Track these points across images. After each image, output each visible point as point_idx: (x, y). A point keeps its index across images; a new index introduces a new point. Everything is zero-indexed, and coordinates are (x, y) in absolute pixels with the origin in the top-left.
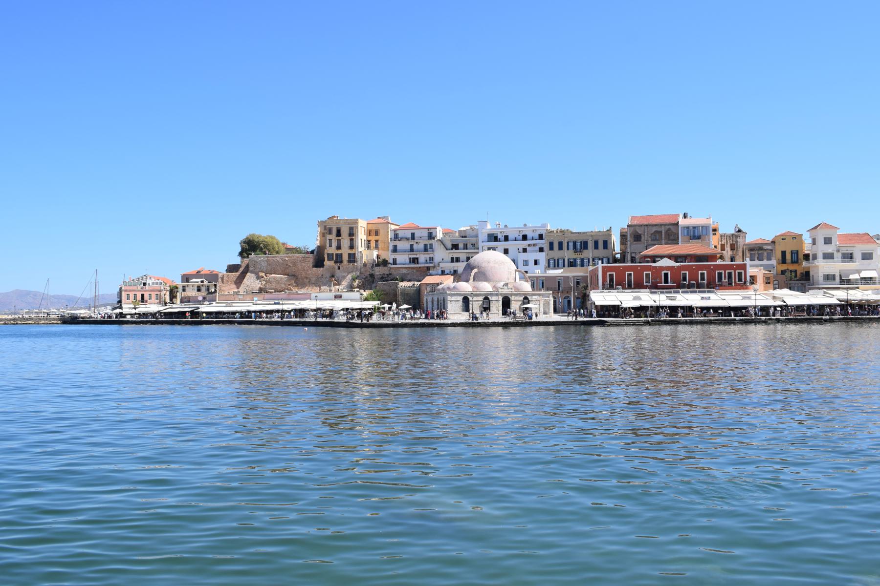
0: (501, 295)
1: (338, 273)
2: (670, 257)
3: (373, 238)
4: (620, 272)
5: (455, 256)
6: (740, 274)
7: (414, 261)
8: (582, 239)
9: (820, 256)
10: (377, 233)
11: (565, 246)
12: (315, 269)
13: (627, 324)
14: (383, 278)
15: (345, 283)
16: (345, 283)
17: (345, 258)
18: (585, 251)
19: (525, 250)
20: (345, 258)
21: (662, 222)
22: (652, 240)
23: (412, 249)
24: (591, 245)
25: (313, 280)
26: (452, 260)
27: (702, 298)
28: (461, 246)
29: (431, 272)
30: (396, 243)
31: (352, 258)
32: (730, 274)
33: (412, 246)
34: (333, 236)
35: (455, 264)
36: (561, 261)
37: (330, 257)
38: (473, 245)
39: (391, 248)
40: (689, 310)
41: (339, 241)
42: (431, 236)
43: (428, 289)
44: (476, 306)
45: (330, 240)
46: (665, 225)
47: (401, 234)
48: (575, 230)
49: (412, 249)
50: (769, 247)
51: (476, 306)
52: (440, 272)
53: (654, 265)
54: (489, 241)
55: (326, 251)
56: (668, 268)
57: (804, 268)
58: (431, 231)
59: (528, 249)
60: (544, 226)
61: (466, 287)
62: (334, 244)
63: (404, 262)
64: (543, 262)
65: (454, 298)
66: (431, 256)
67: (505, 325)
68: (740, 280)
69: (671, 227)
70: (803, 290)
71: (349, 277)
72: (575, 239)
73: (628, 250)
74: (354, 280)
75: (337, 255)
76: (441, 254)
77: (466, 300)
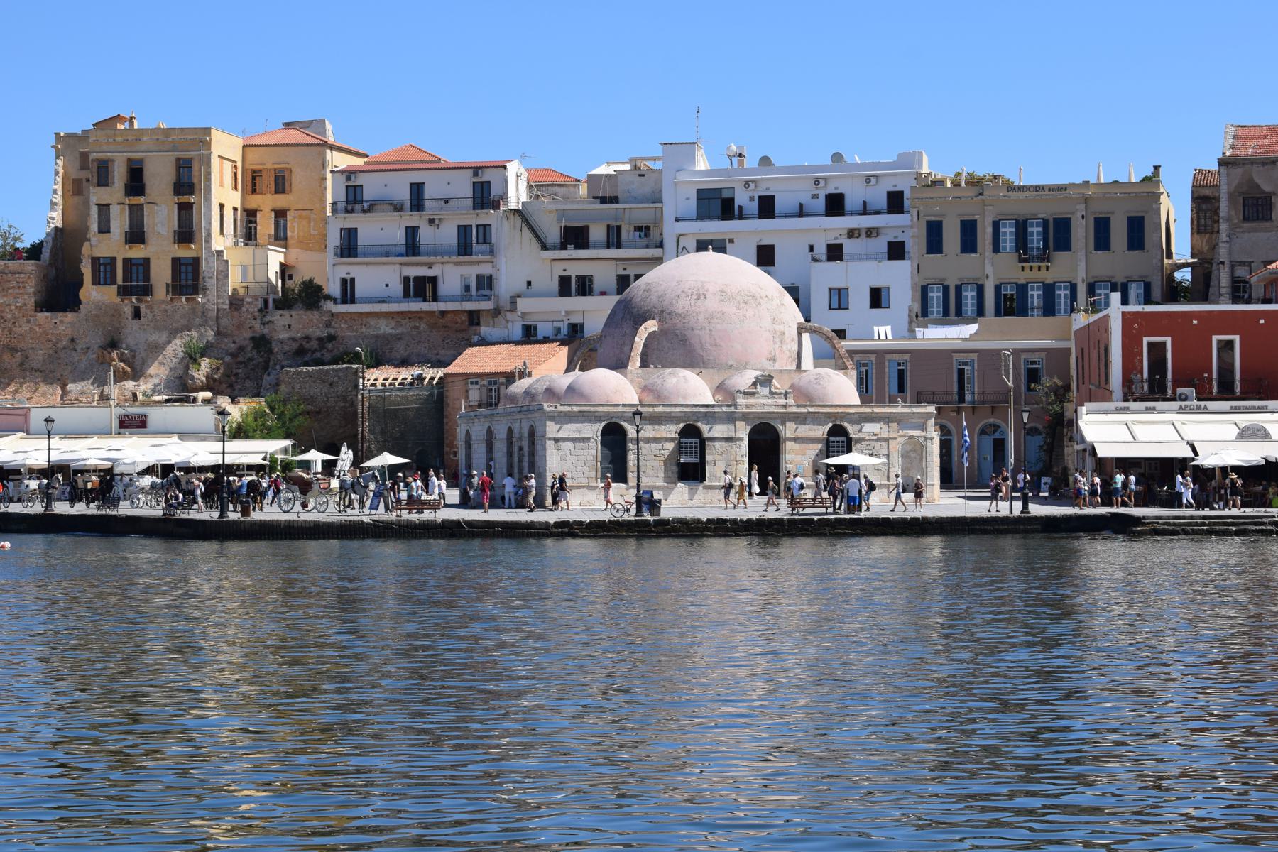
0: (745, 417)
1: (134, 334)
3: (266, 203)
4: (1192, 335)
5: (574, 271)
7: (422, 288)
8: (1049, 210)
10: (281, 183)
12: (43, 316)
13: (1218, 530)
14: (302, 353)
15: (158, 372)
16: (158, 372)
17: (161, 274)
18: (1061, 257)
19: (835, 253)
20: (161, 274)
23: (412, 246)
24: (1081, 233)
25: (38, 356)
26: (565, 287)
28: (597, 233)
29: (484, 330)
31: (188, 277)
33: (412, 232)
34: (114, 194)
35: (576, 304)
36: (969, 295)
38: (643, 230)
39: (334, 239)
41: (136, 214)
42: (485, 195)
43: (475, 395)
44: (651, 457)
47: (372, 188)
49: (412, 246)
51: (651, 457)
52: (517, 332)
54: (700, 217)
55: (86, 249)
58: (486, 176)
59: (849, 246)
60: (908, 160)
61: (614, 388)
62: (119, 222)
63: (385, 292)
64: (902, 298)
65: (569, 430)
66: (486, 270)
71: (176, 346)
72: (1023, 210)
73: (1223, 253)
74: (192, 357)
75: (127, 262)
76: (520, 265)
77: (615, 441)
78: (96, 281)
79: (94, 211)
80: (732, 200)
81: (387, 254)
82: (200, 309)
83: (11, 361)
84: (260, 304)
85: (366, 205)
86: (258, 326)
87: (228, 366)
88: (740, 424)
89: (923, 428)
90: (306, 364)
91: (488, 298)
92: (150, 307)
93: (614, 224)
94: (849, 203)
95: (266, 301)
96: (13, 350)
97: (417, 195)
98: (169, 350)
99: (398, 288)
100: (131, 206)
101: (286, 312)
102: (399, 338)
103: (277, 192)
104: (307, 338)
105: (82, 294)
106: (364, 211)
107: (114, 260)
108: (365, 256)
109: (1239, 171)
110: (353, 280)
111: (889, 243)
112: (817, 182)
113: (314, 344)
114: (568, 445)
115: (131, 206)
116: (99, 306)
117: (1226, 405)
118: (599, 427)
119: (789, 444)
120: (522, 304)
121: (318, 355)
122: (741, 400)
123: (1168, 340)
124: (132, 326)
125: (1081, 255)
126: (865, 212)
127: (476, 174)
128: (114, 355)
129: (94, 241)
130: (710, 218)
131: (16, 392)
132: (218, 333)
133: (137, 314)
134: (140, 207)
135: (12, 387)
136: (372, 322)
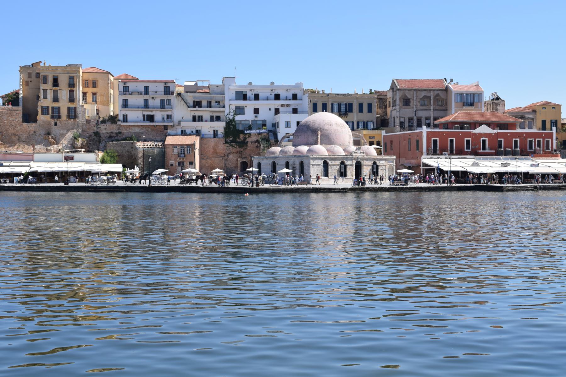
0: (355, 159)
1: (55, 131)
2: (489, 124)
3: (90, 90)
5: (197, 114)
6: (548, 142)
7: (151, 118)
8: (347, 101)
10: (94, 85)
11: (329, 107)
12: (25, 124)
13: (526, 189)
14: (111, 137)
15: (64, 142)
16: (64, 142)
17: (64, 112)
18: (350, 114)
20: (64, 112)
21: (430, 87)
22: (421, 105)
23: (146, 105)
24: (355, 108)
25: (24, 137)
26: (194, 119)
27: (532, 165)
28: (204, 103)
29: (169, 131)
30: (127, 97)
31: (73, 113)
32: (539, 141)
33: (146, 101)
34: (49, 86)
35: (198, 125)
37: (45, 110)
41: (56, 92)
42: (167, 91)
43: (176, 151)
47: (132, 86)
48: (334, 92)
49: (146, 105)
50: (531, 116)
52: (180, 132)
53: (474, 131)
54: (236, 99)
58: (168, 85)
59: (281, 109)
60: (298, 85)
62: (50, 95)
65: (316, 162)
66: (169, 113)
67: (344, 191)
68: (548, 148)
69: (439, 92)
71: (70, 135)
72: (340, 101)
74: (75, 138)
75: (53, 108)
76: (181, 112)
77: (326, 165)
78: (42, 114)
79: (42, 92)
81: (138, 108)
83: (15, 138)
84: (96, 122)
85: (130, 93)
87: (87, 141)
89: (393, 162)
90: (113, 141)
91: (171, 122)
92: (60, 122)
93: (209, 100)
94: (281, 97)
95: (98, 121)
96: (15, 135)
97: (146, 90)
98: (67, 136)
99: (142, 118)
102: (142, 133)
103: (93, 87)
104: (112, 133)
105: (38, 118)
106: (129, 94)
107: (48, 107)
108: (132, 108)
109: (402, 92)
110: (127, 115)
111: (293, 109)
112: (272, 90)
113: (115, 135)
114: (315, 166)
116: (43, 121)
117: (457, 157)
118: (322, 161)
120: (182, 124)
121: (116, 138)
122: (354, 154)
123: (438, 139)
124: (54, 128)
127: (166, 84)
128: (50, 137)
129: (42, 101)
130: (239, 100)
131: (17, 148)
132: (82, 131)
133: (56, 124)
134: (57, 91)
135: (16, 147)
136: (133, 128)
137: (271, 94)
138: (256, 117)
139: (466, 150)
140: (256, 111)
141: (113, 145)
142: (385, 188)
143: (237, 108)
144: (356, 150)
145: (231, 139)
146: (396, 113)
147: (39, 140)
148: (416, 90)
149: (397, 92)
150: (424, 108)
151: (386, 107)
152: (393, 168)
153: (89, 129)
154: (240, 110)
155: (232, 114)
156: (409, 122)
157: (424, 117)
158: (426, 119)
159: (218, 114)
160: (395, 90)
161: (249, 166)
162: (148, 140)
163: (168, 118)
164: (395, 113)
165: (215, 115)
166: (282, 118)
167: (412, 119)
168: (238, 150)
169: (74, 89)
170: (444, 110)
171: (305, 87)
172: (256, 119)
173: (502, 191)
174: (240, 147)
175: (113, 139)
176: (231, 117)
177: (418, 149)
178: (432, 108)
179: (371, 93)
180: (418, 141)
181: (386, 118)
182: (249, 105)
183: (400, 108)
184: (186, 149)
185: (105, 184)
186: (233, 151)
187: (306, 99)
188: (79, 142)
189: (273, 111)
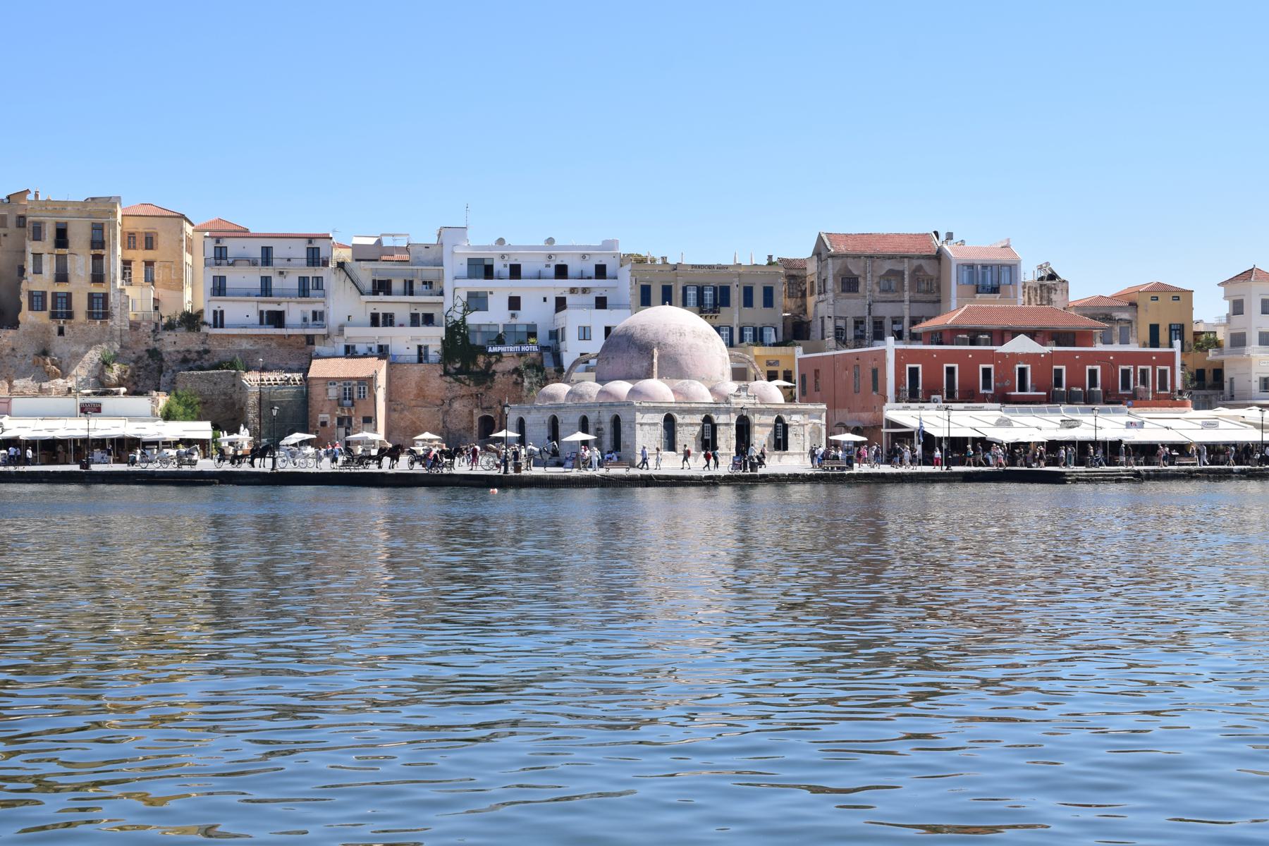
0: (735, 411)
1: (60, 346)
2: (1032, 334)
3: (139, 256)
5: (381, 310)
6: (1163, 373)
7: (276, 319)
9: (1253, 337)
10: (150, 243)
11: (677, 294)
14: (186, 361)
15: (81, 372)
16: (81, 372)
17: (80, 305)
18: (723, 309)
20: (80, 305)
21: (901, 250)
22: (882, 291)
23: (266, 289)
24: (736, 296)
26: (375, 321)
27: (1130, 425)
28: (397, 285)
29: (318, 348)
30: (223, 271)
31: (100, 307)
32: (1144, 372)
33: (266, 281)
34: (46, 246)
35: (382, 334)
37: (37, 301)
40: (1112, 449)
42: (314, 258)
43: (333, 392)
45: (38, 256)
46: (910, 257)
47: (234, 247)
48: (688, 261)
49: (266, 289)
50: (1125, 316)
52: (342, 350)
54: (470, 277)
56: (1027, 357)
57: (1212, 362)
58: (316, 244)
59: (570, 299)
60: (609, 245)
62: (49, 267)
63: (247, 321)
65: (648, 418)
66: (319, 307)
67: (711, 483)
68: (1163, 387)
69: (922, 262)
70: (1210, 408)
71: (93, 356)
72: (701, 281)
74: (105, 363)
75: (55, 295)
76: (344, 305)
77: (670, 423)
78: (31, 308)
79: (30, 258)
80: (492, 266)
81: (248, 295)
82: (108, 329)
84: (153, 327)
85: (231, 261)
86: (151, 342)
87: (132, 369)
88: (732, 415)
89: (820, 418)
90: (191, 369)
92: (72, 327)
93: (409, 279)
94: (570, 271)
95: (157, 325)
97: (267, 256)
98: (87, 357)
99: (256, 319)
100: (57, 255)
101: (172, 333)
102: (257, 352)
104: (189, 351)
105: (20, 317)
106: (229, 265)
107: (44, 294)
108: (233, 295)
109: (840, 261)
110: (222, 312)
112: (550, 257)
113: (194, 356)
115: (57, 255)
116: (33, 325)
117: (962, 406)
119: (757, 428)
121: (198, 363)
122: (733, 400)
123: (920, 366)
125: (736, 309)
126: (582, 277)
127: (310, 242)
128: (48, 360)
129: (30, 279)
130: (476, 277)
132: (122, 347)
133: (61, 332)
136: (237, 341)
137: (548, 266)
138: (513, 316)
139: (982, 391)
140: (514, 303)
141: (190, 380)
142: (803, 475)
143: (471, 295)
144: (739, 390)
145: (458, 365)
146: (825, 309)
147: (23, 367)
148: (871, 257)
149: (830, 260)
150: (890, 296)
151: (804, 295)
152: (820, 431)
153: (137, 342)
154: (477, 301)
155: (460, 309)
156: (856, 328)
157: (888, 316)
158: (894, 322)
159: (428, 310)
160: (823, 256)
161: (497, 426)
162: (270, 367)
163: (315, 318)
164: (823, 308)
165: (421, 311)
166: (572, 320)
167: (862, 322)
168: (474, 389)
169: (104, 252)
170: (934, 302)
171: (624, 249)
172: (514, 321)
173: (1064, 482)
174: (477, 384)
175: (191, 365)
176: (458, 317)
177: (875, 388)
178: (907, 296)
179: (771, 264)
180: (875, 372)
181: (805, 318)
182: (499, 290)
183: (836, 296)
184: (356, 389)
185: (172, 467)
186: (463, 392)
187: (625, 274)
188: (115, 372)
189: (552, 303)
